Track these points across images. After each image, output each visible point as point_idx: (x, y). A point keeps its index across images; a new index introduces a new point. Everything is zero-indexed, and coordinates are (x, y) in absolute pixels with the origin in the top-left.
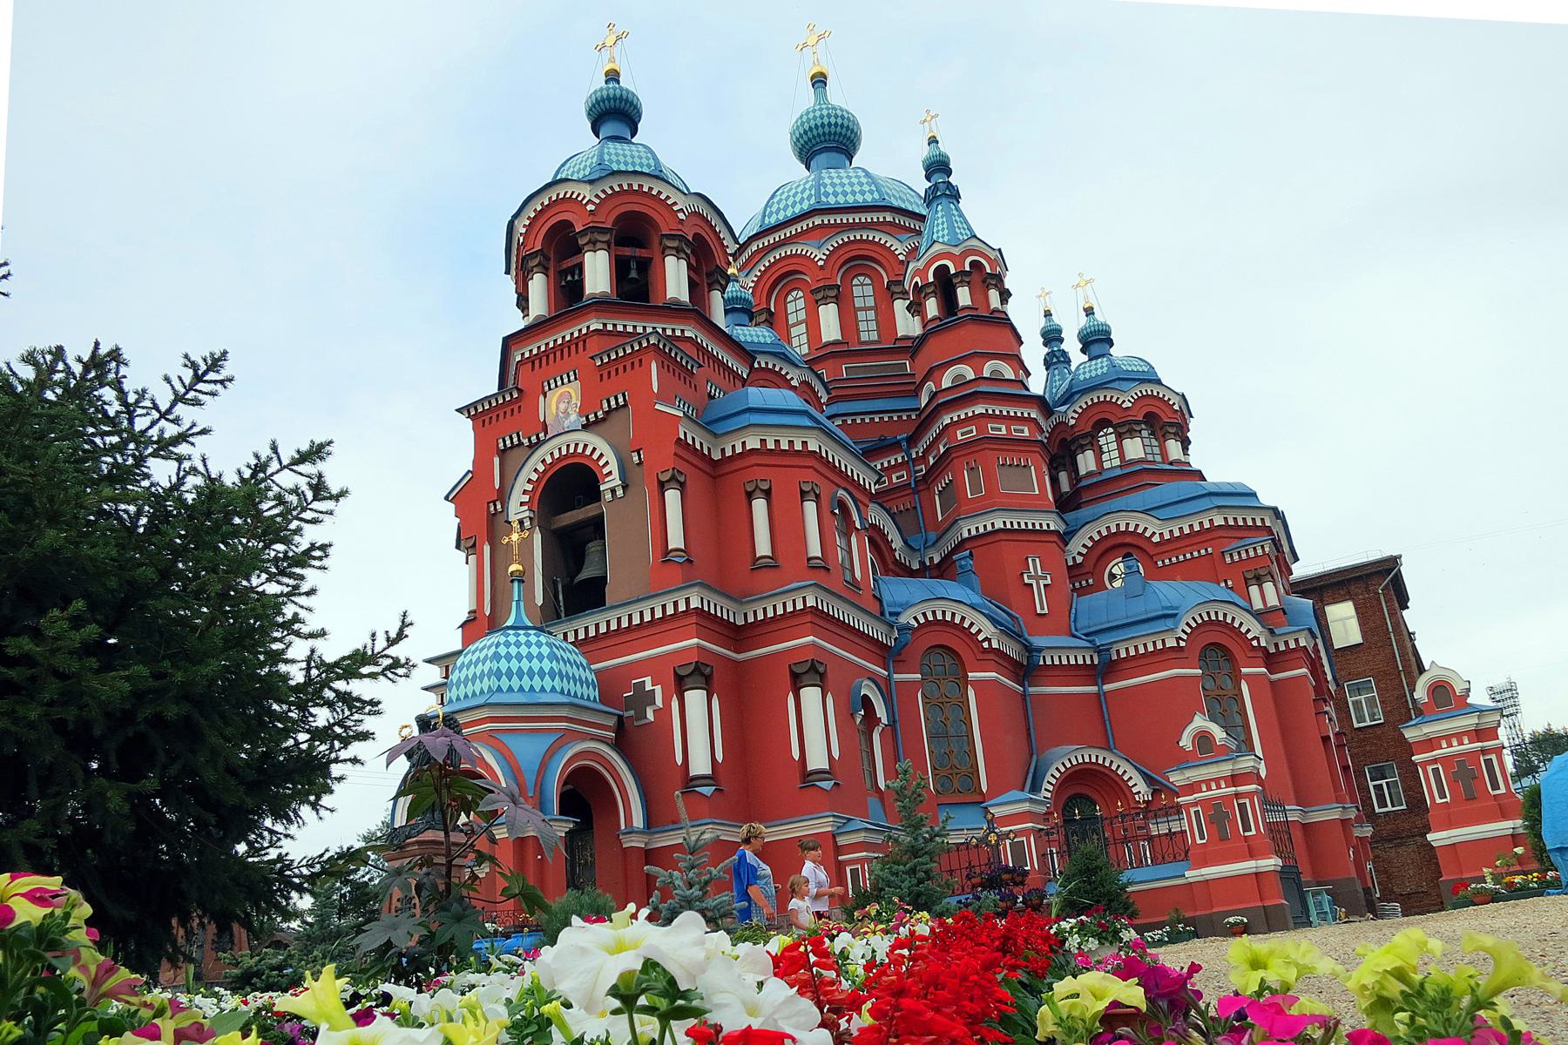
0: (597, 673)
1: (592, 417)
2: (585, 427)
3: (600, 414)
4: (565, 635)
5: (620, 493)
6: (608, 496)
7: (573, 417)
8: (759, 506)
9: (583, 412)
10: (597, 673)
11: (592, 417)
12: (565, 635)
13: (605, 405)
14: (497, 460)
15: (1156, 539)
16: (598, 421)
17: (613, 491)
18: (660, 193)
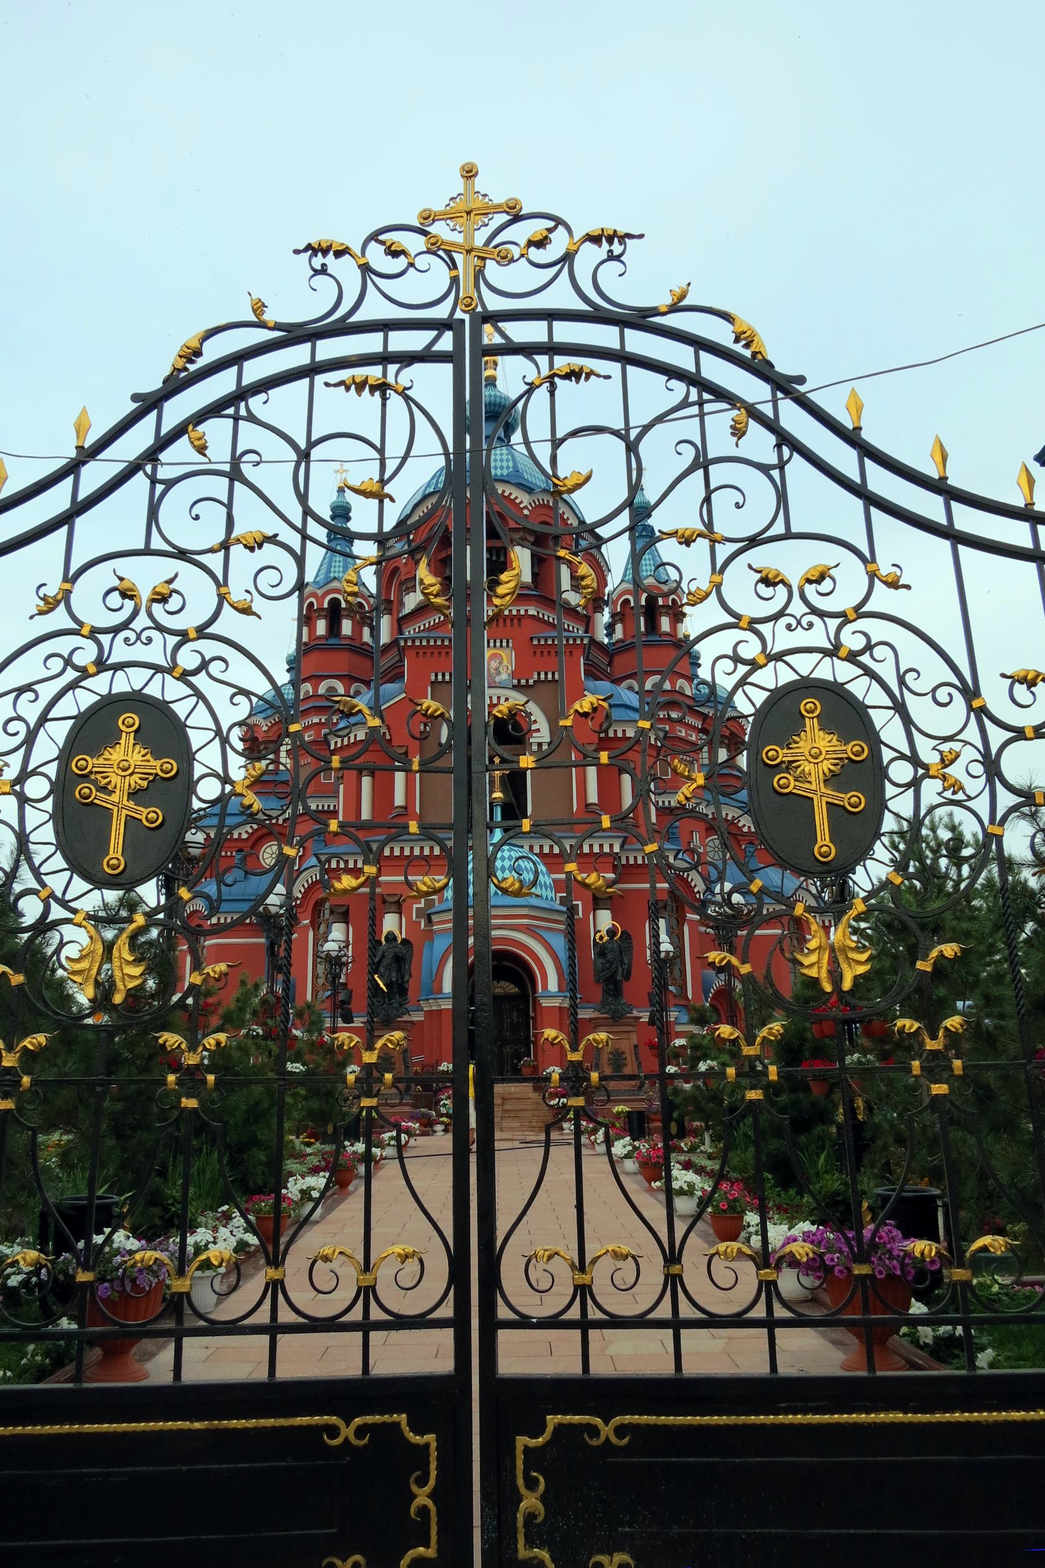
0: (554, 881)
1: (515, 682)
2: (515, 687)
3: (531, 682)
4: (531, 847)
5: (545, 747)
6: (535, 748)
7: (504, 676)
8: (626, 779)
9: (514, 675)
10: (554, 881)
11: (523, 682)
12: (531, 847)
13: (536, 677)
14: (429, 689)
15: (745, 829)
16: (527, 686)
17: (540, 745)
18: (510, 494)
